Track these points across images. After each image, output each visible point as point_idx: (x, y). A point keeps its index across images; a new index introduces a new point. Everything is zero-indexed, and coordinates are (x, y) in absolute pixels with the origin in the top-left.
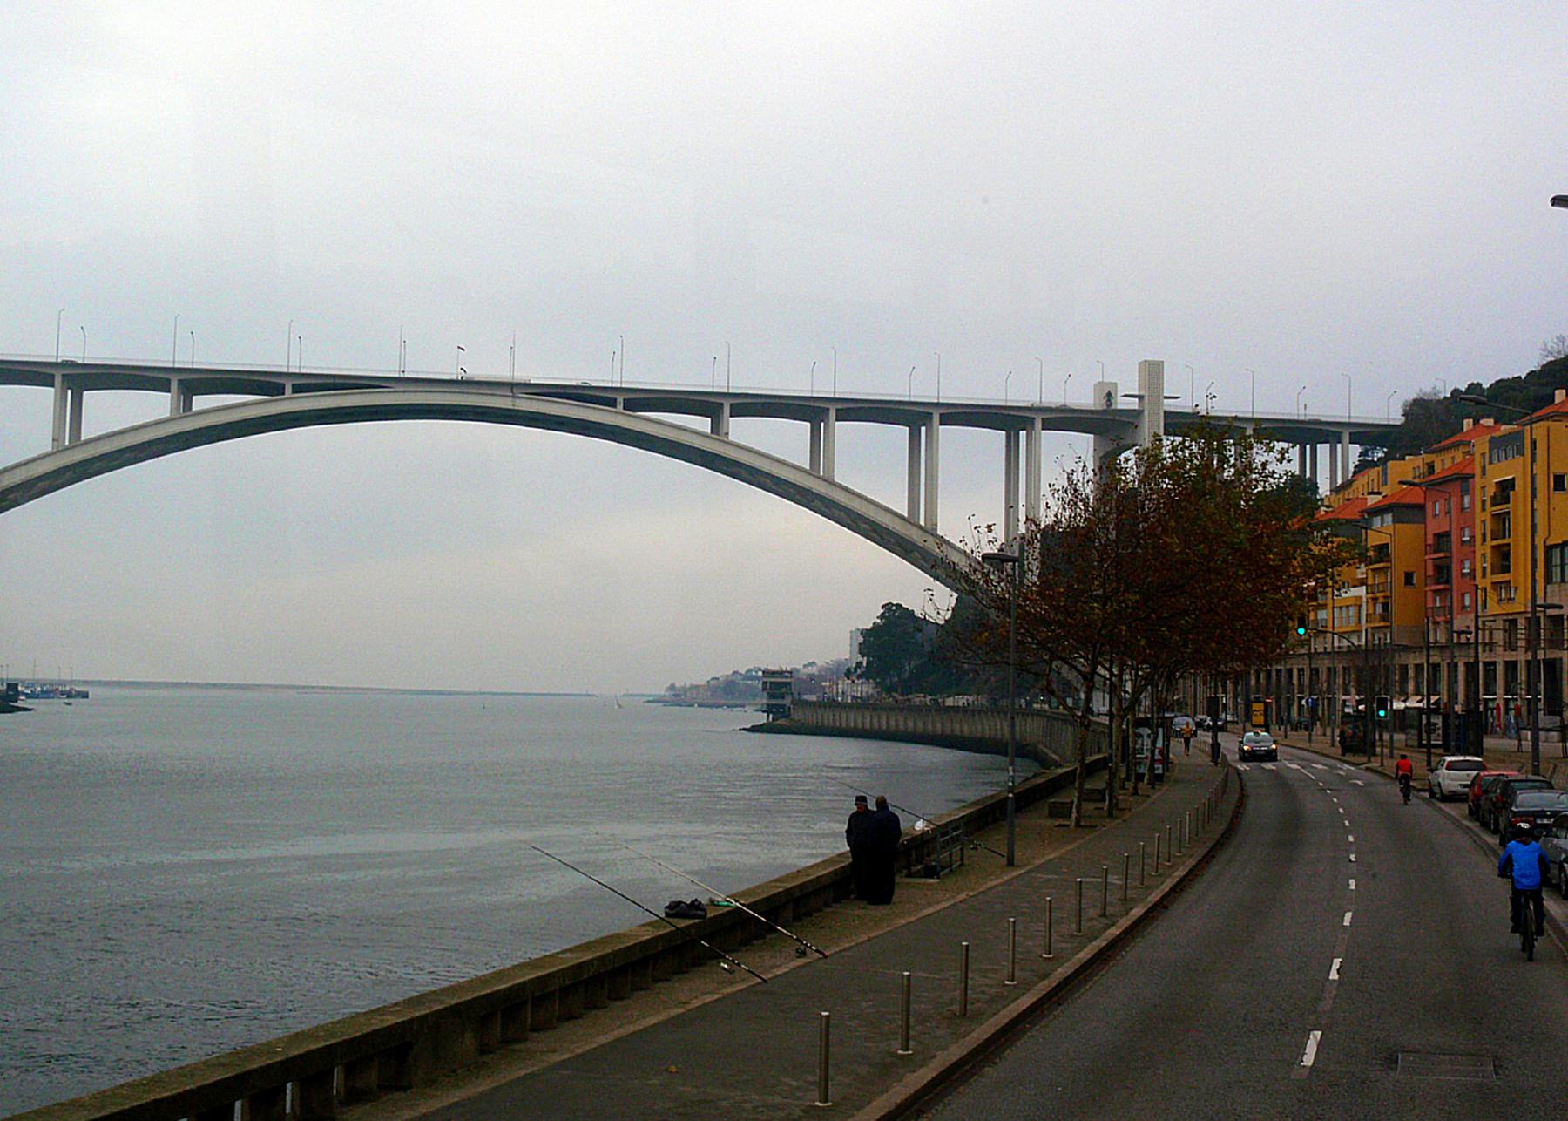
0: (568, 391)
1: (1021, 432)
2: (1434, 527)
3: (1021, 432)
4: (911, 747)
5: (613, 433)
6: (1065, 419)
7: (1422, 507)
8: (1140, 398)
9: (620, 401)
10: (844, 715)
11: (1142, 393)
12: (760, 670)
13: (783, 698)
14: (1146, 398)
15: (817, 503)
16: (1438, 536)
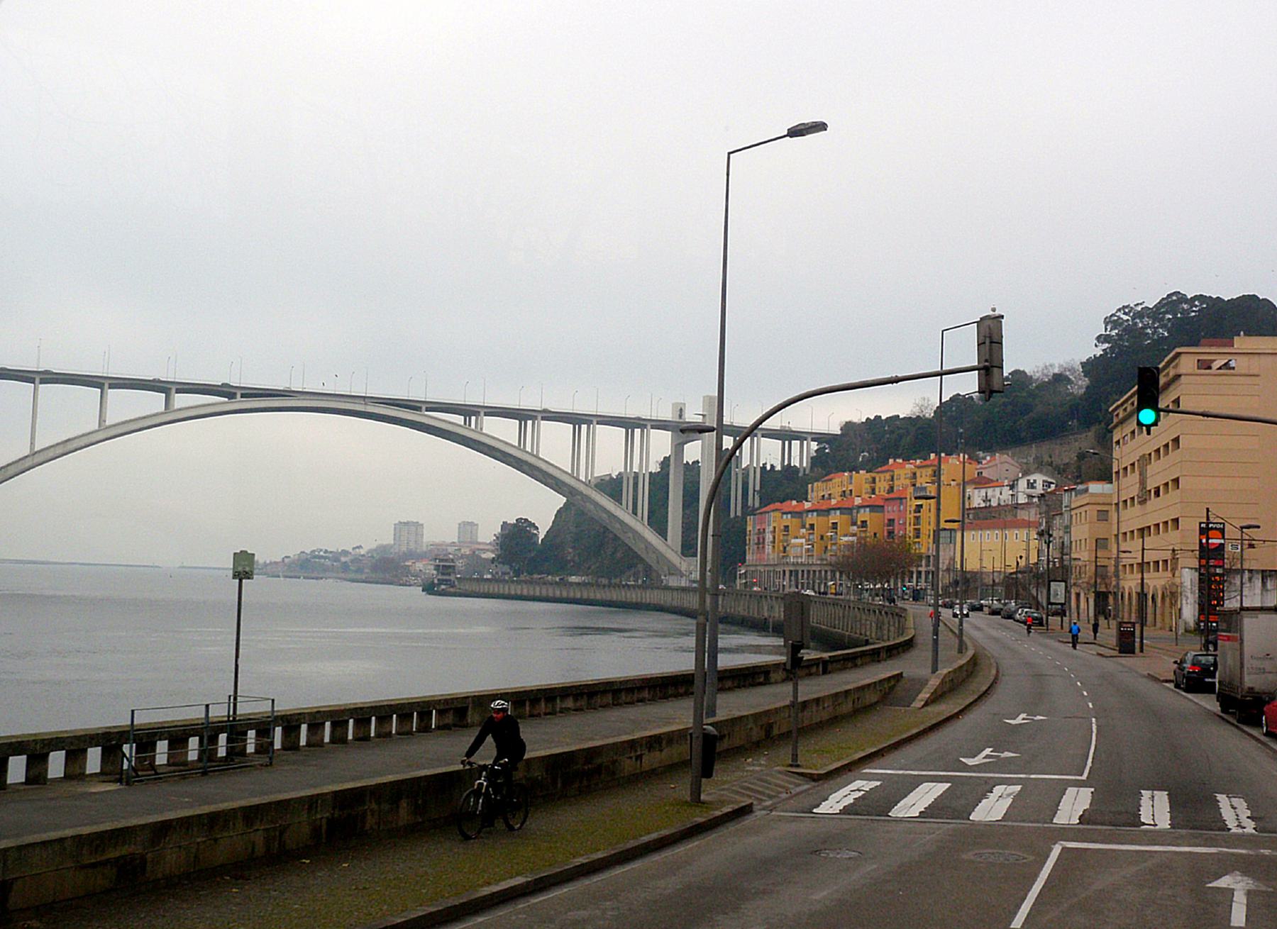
0: (398, 402)
1: (636, 430)
2: (888, 516)
3: (636, 430)
4: (530, 603)
5: (428, 429)
6: (661, 425)
7: (883, 507)
8: (704, 416)
9: (424, 408)
10: (501, 586)
11: (705, 413)
12: (321, 550)
13: (449, 574)
14: (707, 417)
15: (525, 467)
16: (889, 520)
